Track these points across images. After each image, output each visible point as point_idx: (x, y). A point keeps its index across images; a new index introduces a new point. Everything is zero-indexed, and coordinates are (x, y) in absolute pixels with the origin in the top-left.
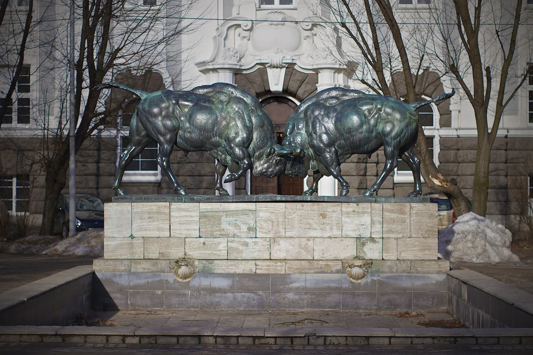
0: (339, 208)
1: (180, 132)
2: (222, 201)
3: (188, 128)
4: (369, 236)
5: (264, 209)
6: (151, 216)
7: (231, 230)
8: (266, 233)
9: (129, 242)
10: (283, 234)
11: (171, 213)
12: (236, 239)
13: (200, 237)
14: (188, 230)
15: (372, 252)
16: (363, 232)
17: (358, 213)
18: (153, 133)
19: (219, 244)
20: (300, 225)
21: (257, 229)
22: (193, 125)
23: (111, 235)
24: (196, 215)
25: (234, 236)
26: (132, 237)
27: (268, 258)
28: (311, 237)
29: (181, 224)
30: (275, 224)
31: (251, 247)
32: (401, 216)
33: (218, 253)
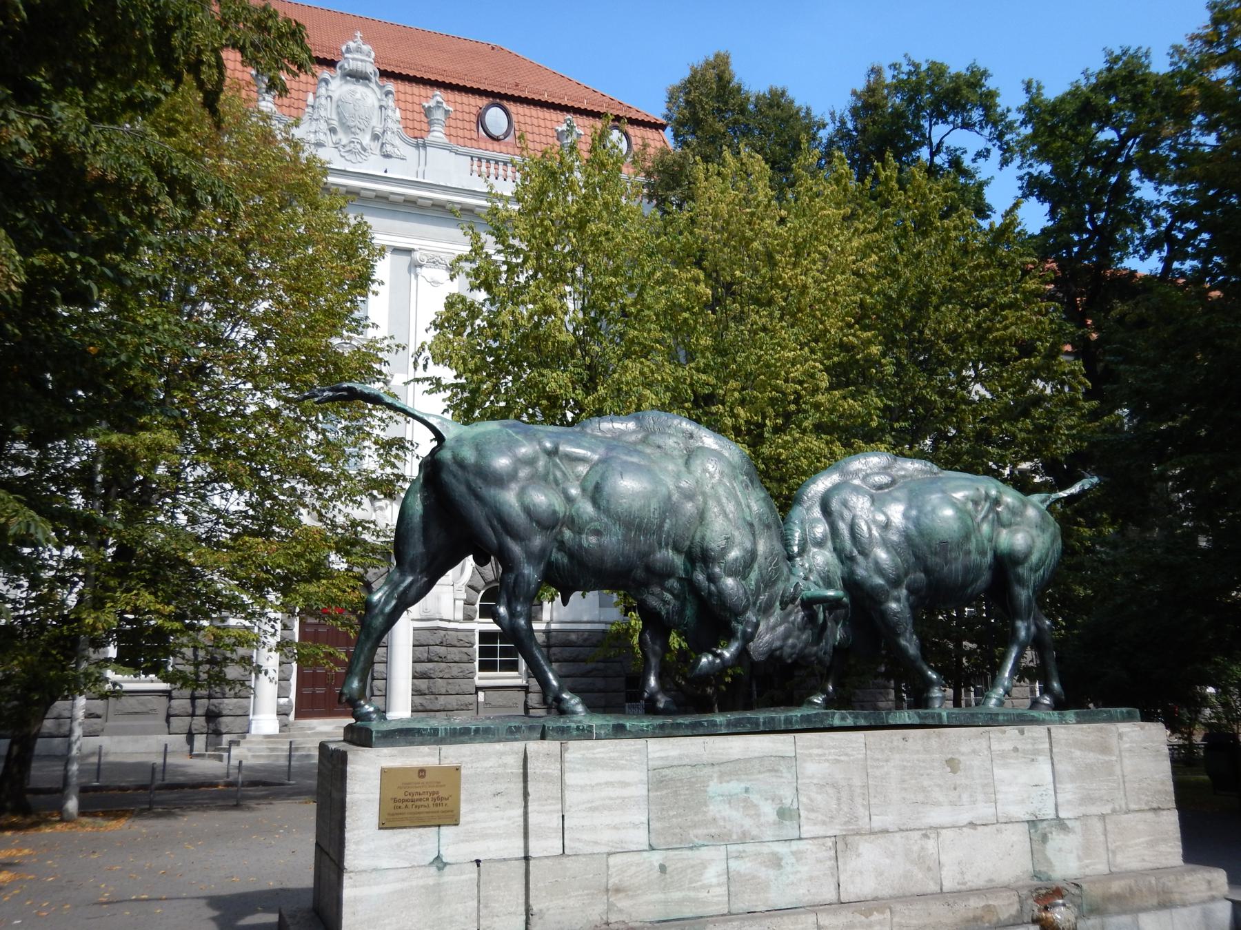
0: (984, 743)
1: (567, 534)
3: (592, 520)
4: (1052, 816)
5: (816, 751)
6: (501, 787)
7: (733, 816)
8: (824, 823)
9: (431, 881)
10: (864, 824)
12: (750, 848)
13: (652, 848)
14: (616, 828)
15: (1066, 860)
16: (1040, 806)
17: (1025, 752)
19: (704, 865)
21: (802, 813)
22: (607, 512)
24: (637, 775)
25: (744, 838)
26: (439, 863)
28: (931, 828)
29: (593, 809)
31: (789, 869)
32: (1107, 758)
33: (703, 895)
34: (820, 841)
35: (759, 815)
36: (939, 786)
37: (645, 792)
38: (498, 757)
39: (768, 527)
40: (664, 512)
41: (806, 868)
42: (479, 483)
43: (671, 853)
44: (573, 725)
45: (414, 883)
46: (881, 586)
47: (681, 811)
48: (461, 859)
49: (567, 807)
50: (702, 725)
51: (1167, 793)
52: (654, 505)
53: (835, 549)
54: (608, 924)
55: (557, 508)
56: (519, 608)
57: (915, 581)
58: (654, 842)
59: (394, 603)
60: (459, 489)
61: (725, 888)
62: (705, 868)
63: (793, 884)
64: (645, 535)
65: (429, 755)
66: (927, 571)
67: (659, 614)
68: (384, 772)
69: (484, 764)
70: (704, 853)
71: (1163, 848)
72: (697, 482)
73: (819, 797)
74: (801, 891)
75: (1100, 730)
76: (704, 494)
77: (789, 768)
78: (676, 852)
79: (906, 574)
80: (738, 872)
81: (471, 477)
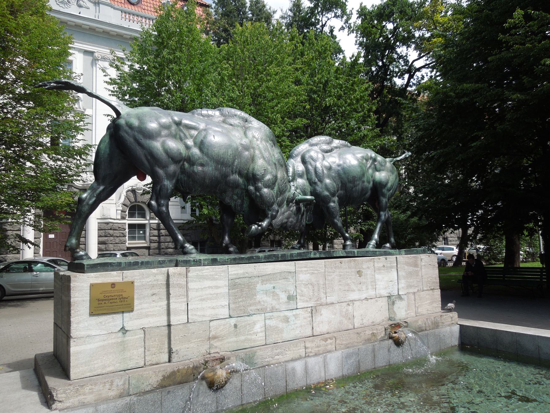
1: (186, 165)
2: (253, 261)
3: (199, 158)
4: (397, 294)
6: (155, 291)
8: (307, 301)
9: (119, 340)
10: (324, 300)
11: (189, 284)
12: (275, 314)
13: (230, 317)
14: (213, 308)
15: (402, 312)
18: (146, 162)
19: (254, 323)
20: (340, 287)
21: (298, 297)
23: (83, 333)
24: (223, 283)
26: (123, 330)
27: (311, 334)
29: (204, 300)
30: (316, 288)
31: (292, 323)
32: (416, 269)
33: (254, 337)
34: (305, 309)
35: (279, 299)
36: (354, 283)
37: (227, 291)
38: (156, 275)
39: (282, 166)
40: (235, 156)
41: (299, 322)
42: (140, 137)
43: (239, 318)
44: (191, 259)
45: (110, 342)
46: (328, 196)
47: (244, 299)
48: (135, 328)
49: (190, 299)
50: (253, 258)
51: (437, 283)
52: (230, 152)
53: (308, 179)
54: (210, 354)
55: (182, 151)
56: (162, 202)
57: (341, 194)
58: (231, 314)
59: (94, 199)
60: (130, 140)
61: (264, 333)
62: (255, 324)
63: (293, 329)
64: (226, 167)
65: (116, 276)
66: (346, 190)
67: (230, 206)
68: (92, 286)
69: (146, 280)
70: (254, 318)
71: (435, 305)
72: (250, 142)
73: (305, 290)
74: (297, 332)
75: (414, 257)
76: (253, 148)
77: (292, 277)
78: (242, 318)
79: (338, 191)
80: (270, 326)
81: (136, 134)
